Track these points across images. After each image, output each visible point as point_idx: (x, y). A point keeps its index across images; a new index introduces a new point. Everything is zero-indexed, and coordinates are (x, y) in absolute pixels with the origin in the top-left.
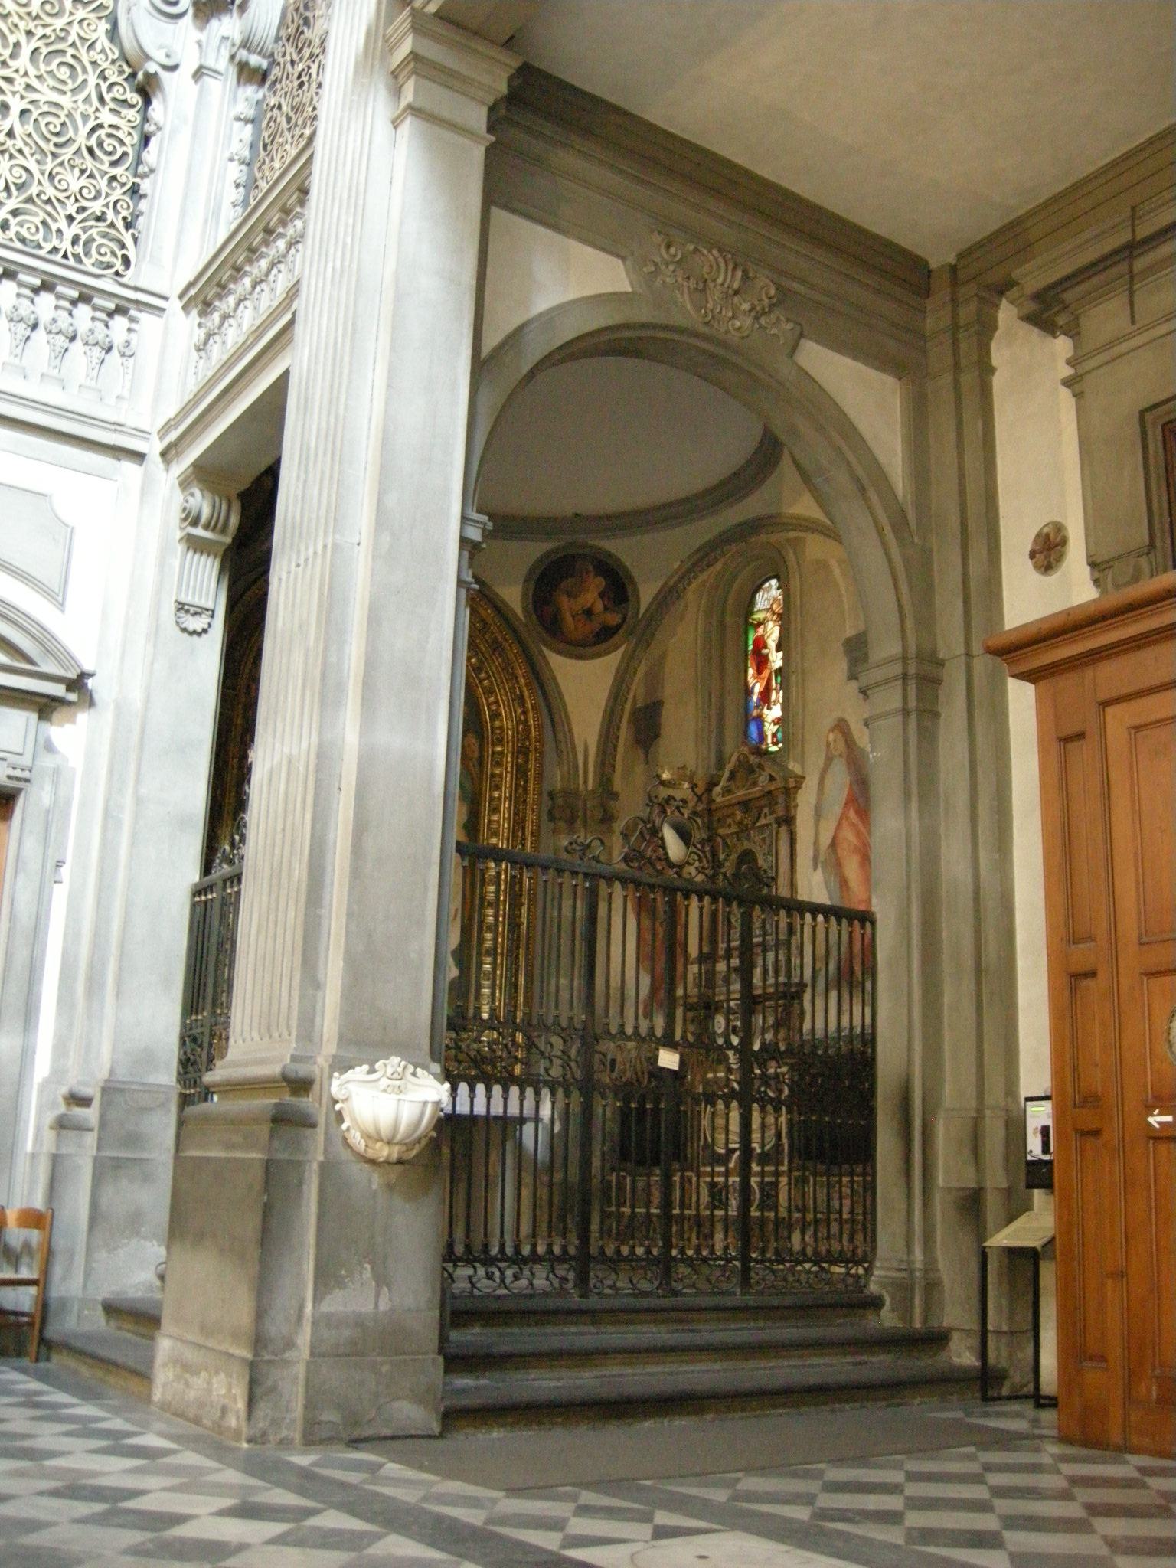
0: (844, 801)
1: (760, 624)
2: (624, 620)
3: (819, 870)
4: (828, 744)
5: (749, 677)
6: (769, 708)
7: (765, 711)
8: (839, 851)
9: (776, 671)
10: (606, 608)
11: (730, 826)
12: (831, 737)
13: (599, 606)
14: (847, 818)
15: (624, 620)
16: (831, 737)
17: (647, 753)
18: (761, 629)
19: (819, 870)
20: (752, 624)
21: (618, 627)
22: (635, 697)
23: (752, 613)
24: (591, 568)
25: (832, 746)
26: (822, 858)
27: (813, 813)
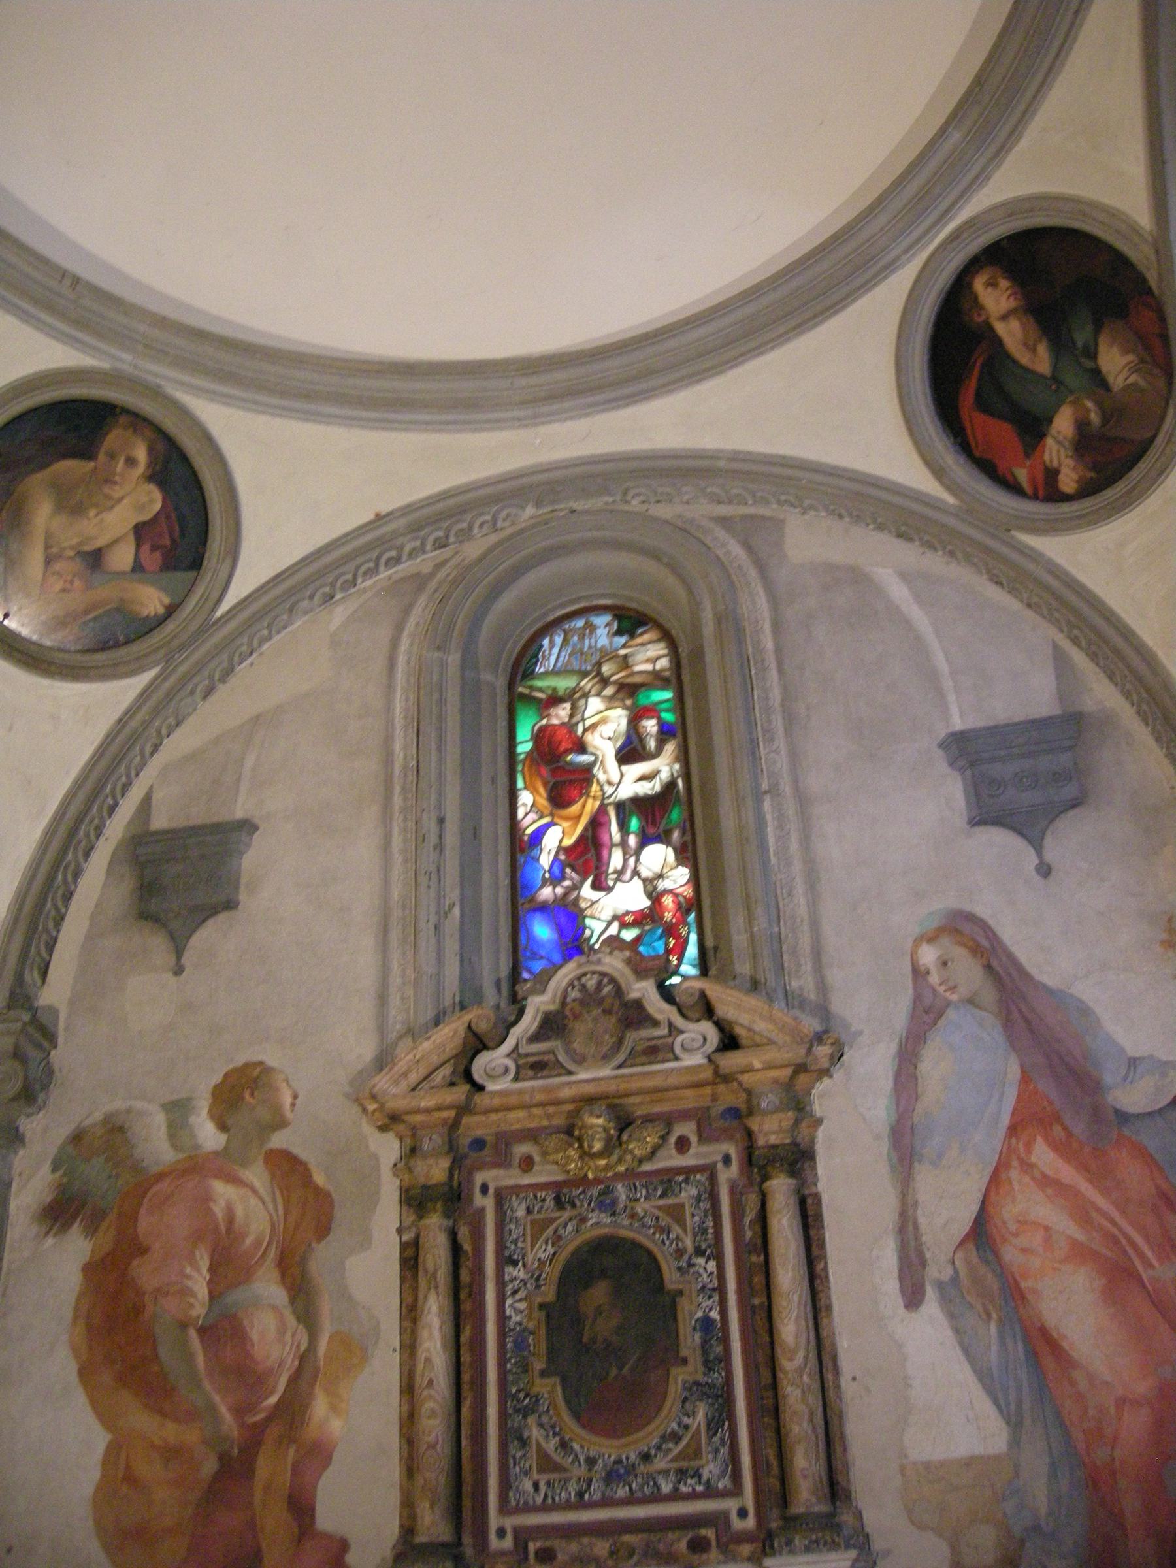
0: (1005, 1120)
1: (555, 700)
2: (171, 611)
3: (931, 1306)
4: (919, 974)
5: (521, 813)
6: (596, 886)
7: (587, 891)
8: (1010, 1254)
9: (620, 806)
10: (138, 567)
11: (527, 1164)
12: (928, 956)
13: (123, 557)
14: (1027, 1167)
15: (171, 611)
16: (928, 956)
17: (179, 952)
18: (561, 713)
19: (931, 1306)
20: (528, 699)
21: (161, 621)
22: (147, 800)
23: (529, 674)
24: (141, 454)
25: (934, 979)
26: (938, 1269)
27: (885, 1146)
